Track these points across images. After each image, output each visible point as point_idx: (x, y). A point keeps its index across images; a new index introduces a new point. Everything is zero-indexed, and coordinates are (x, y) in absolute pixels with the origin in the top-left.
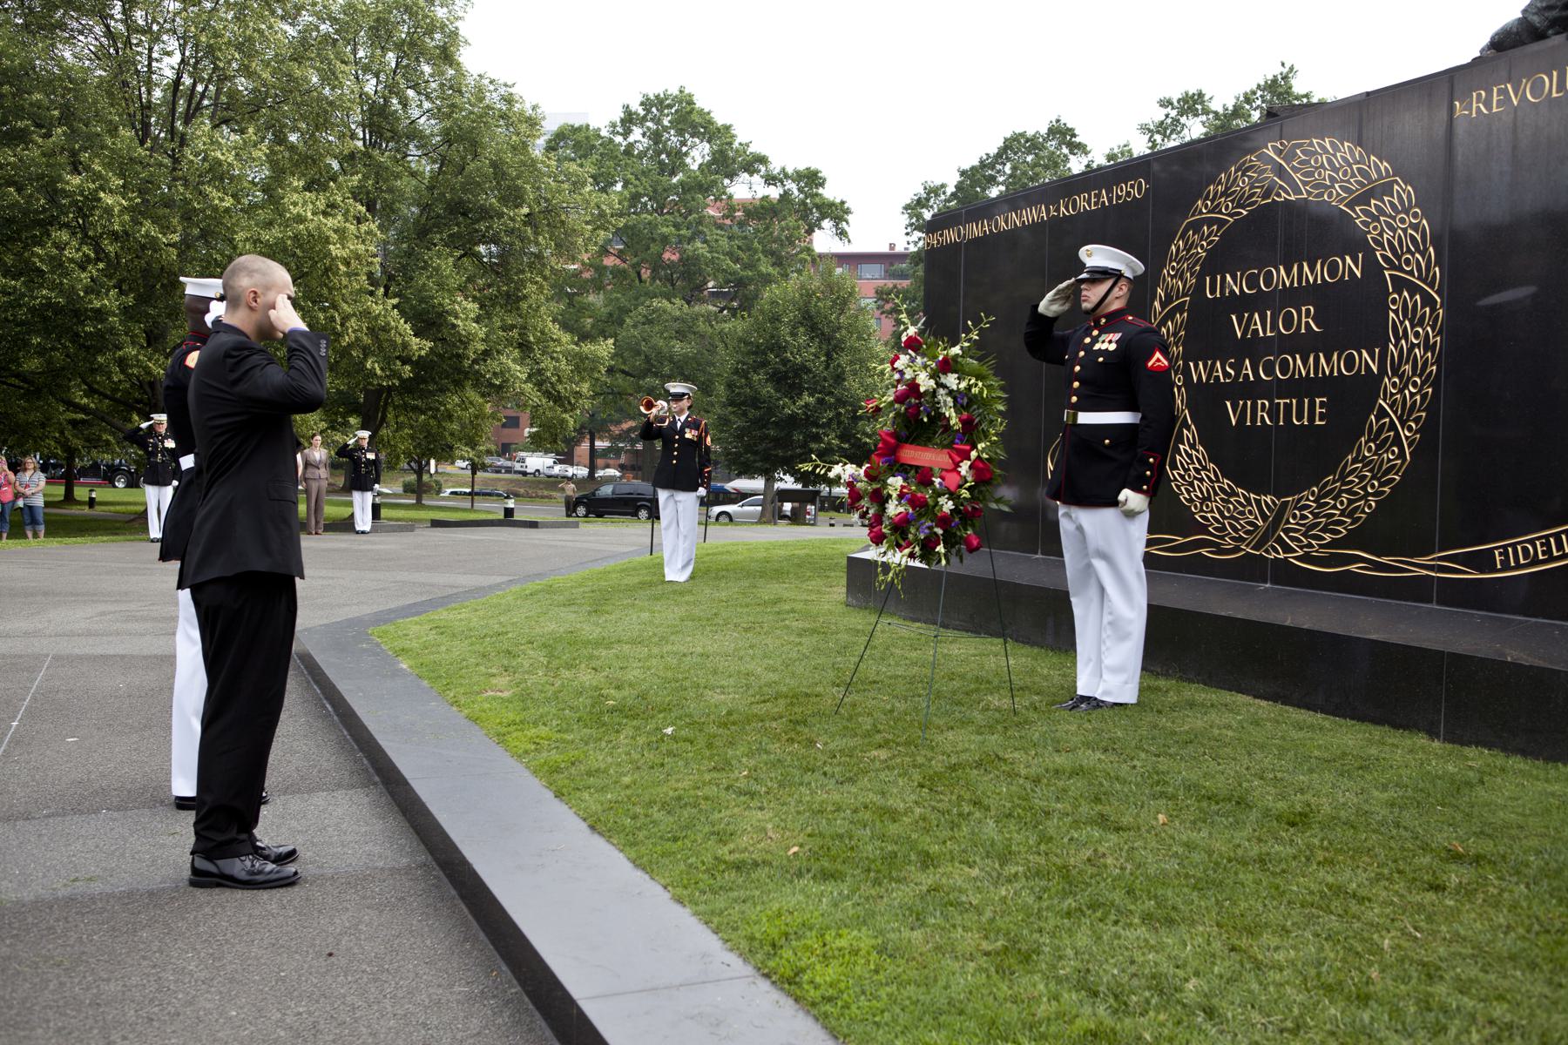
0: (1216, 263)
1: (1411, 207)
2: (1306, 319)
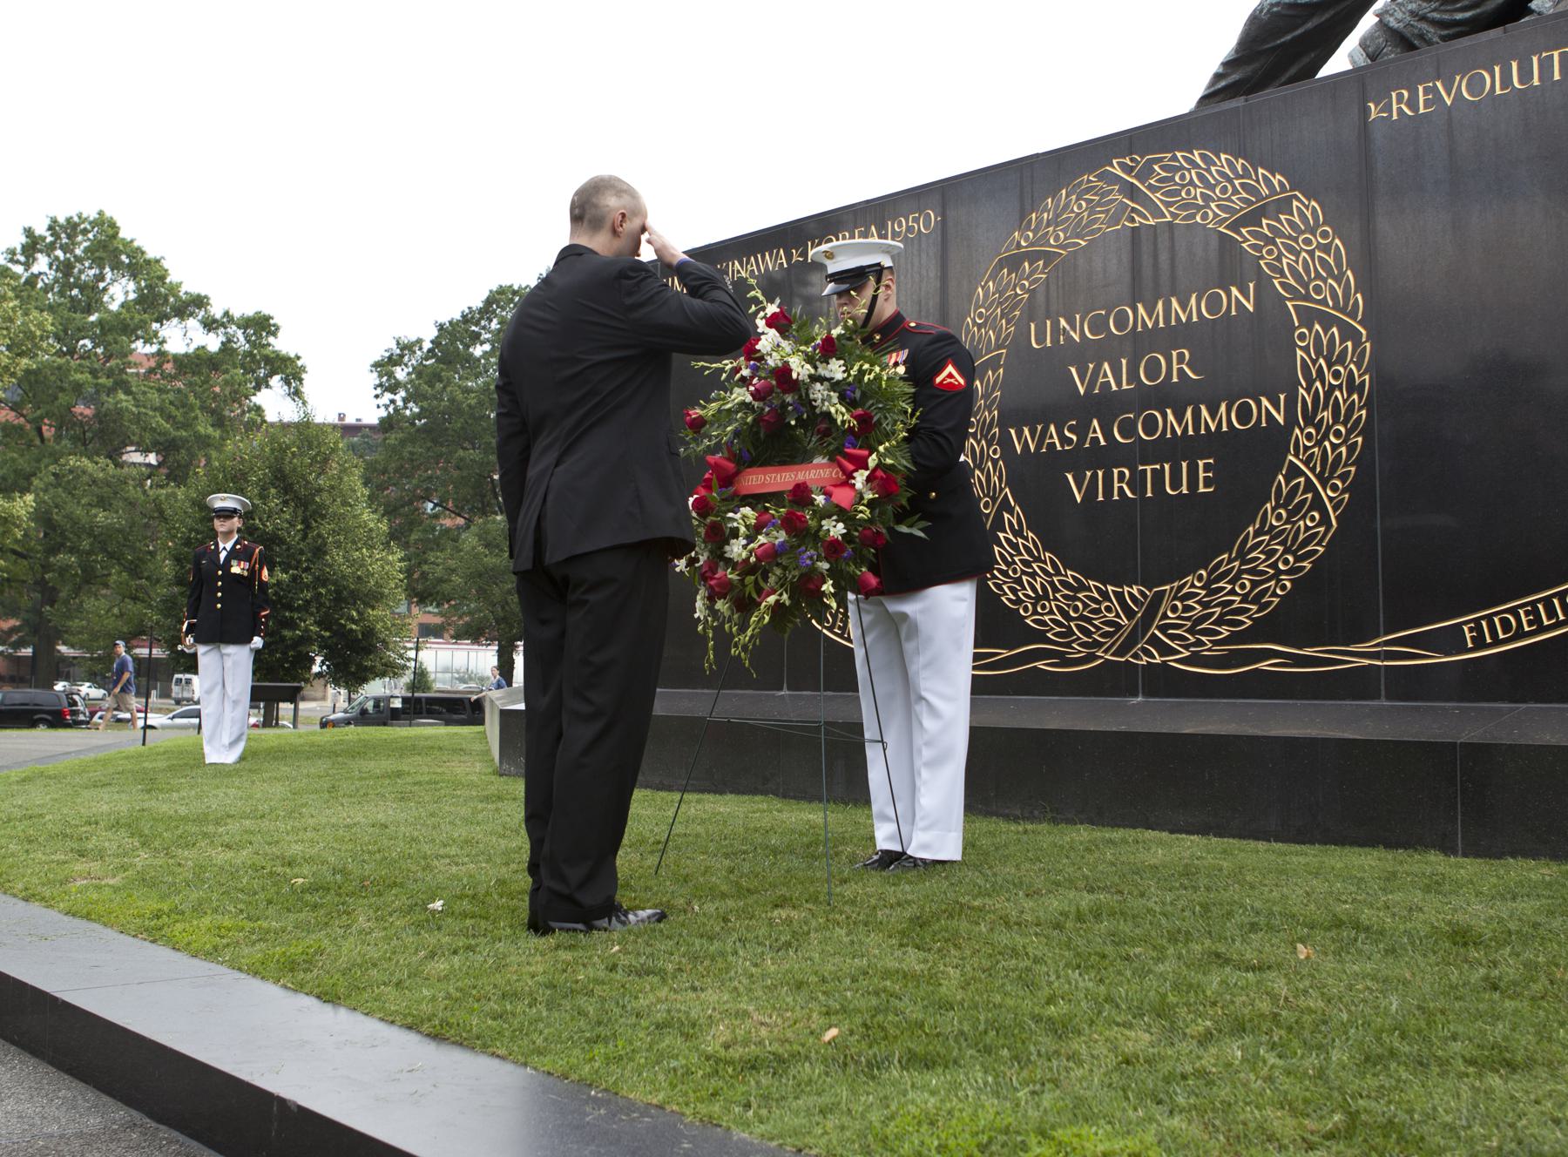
1: (1317, 225)
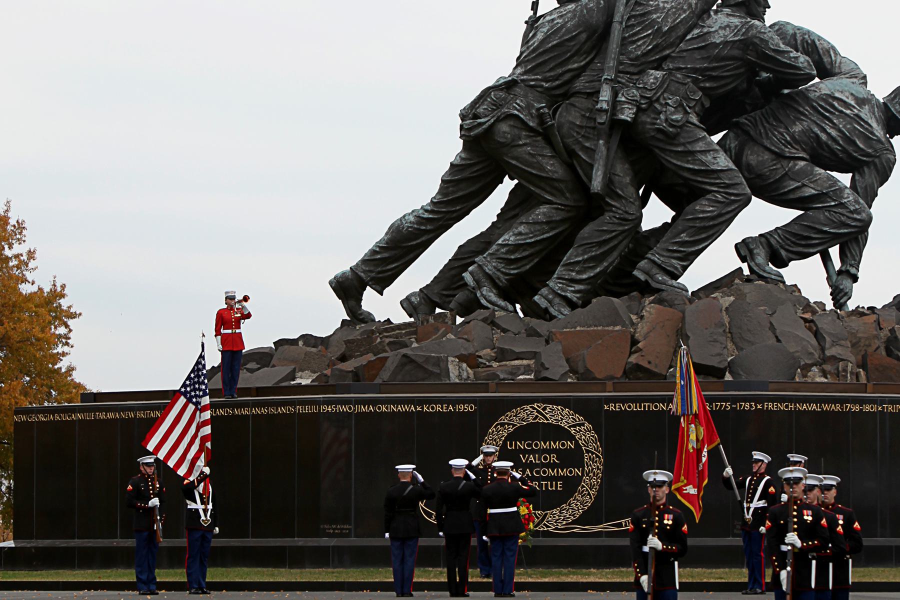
0: (510, 437)
2: (554, 458)
